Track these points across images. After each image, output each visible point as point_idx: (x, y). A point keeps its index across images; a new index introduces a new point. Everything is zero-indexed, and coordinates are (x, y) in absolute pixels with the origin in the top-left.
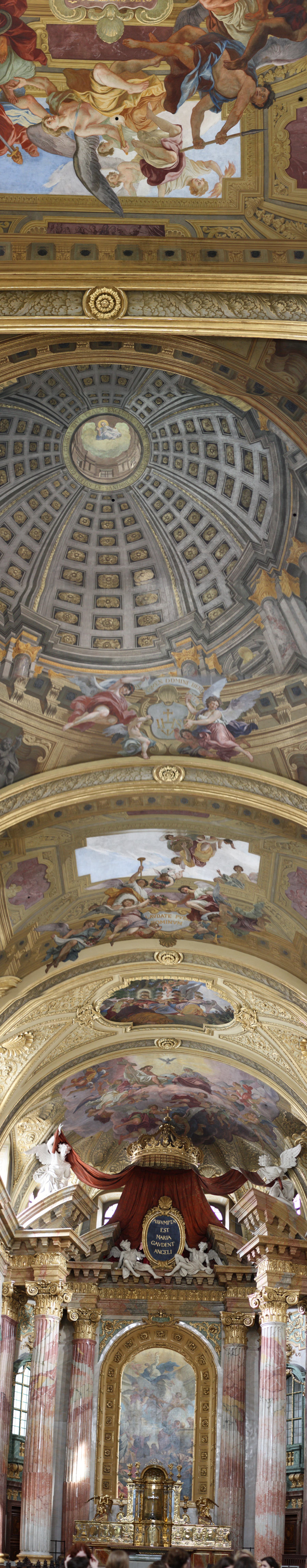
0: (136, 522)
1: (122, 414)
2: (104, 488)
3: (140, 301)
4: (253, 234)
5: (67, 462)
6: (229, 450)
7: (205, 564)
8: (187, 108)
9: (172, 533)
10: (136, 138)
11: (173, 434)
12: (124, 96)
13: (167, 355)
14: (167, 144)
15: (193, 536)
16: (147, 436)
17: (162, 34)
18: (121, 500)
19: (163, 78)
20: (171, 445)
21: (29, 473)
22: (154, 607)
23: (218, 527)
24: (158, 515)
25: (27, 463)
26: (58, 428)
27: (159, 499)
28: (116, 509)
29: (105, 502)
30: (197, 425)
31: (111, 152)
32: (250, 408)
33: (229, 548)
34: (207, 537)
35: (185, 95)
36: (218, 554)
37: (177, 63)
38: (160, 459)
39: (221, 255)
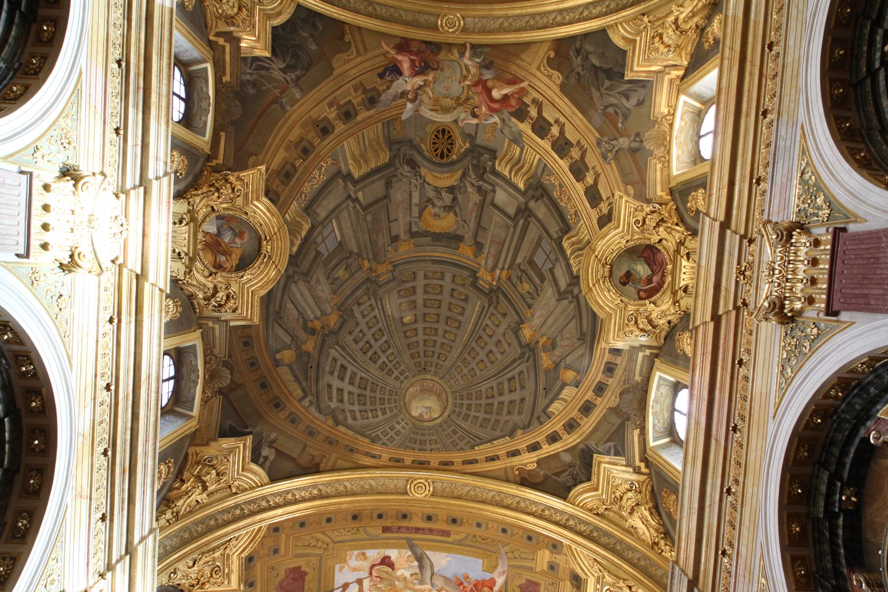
0: (411, 355)
1: (415, 421)
2: (429, 377)
3: (399, 488)
4: (330, 533)
5: (450, 395)
6: (351, 401)
7: (370, 328)
9: (389, 347)
11: (385, 409)
14: (378, 579)
15: (376, 346)
16: (401, 407)
18: (419, 369)
20: (386, 402)
21: (473, 391)
22: (403, 300)
23: (360, 352)
24: (397, 359)
25: (474, 398)
26: (453, 417)
27: (396, 369)
28: (423, 363)
29: (429, 368)
30: (370, 415)
31: (412, 575)
32: (337, 428)
33: (354, 340)
34: (367, 345)
36: (361, 335)
38: (394, 393)
39: (350, 517)
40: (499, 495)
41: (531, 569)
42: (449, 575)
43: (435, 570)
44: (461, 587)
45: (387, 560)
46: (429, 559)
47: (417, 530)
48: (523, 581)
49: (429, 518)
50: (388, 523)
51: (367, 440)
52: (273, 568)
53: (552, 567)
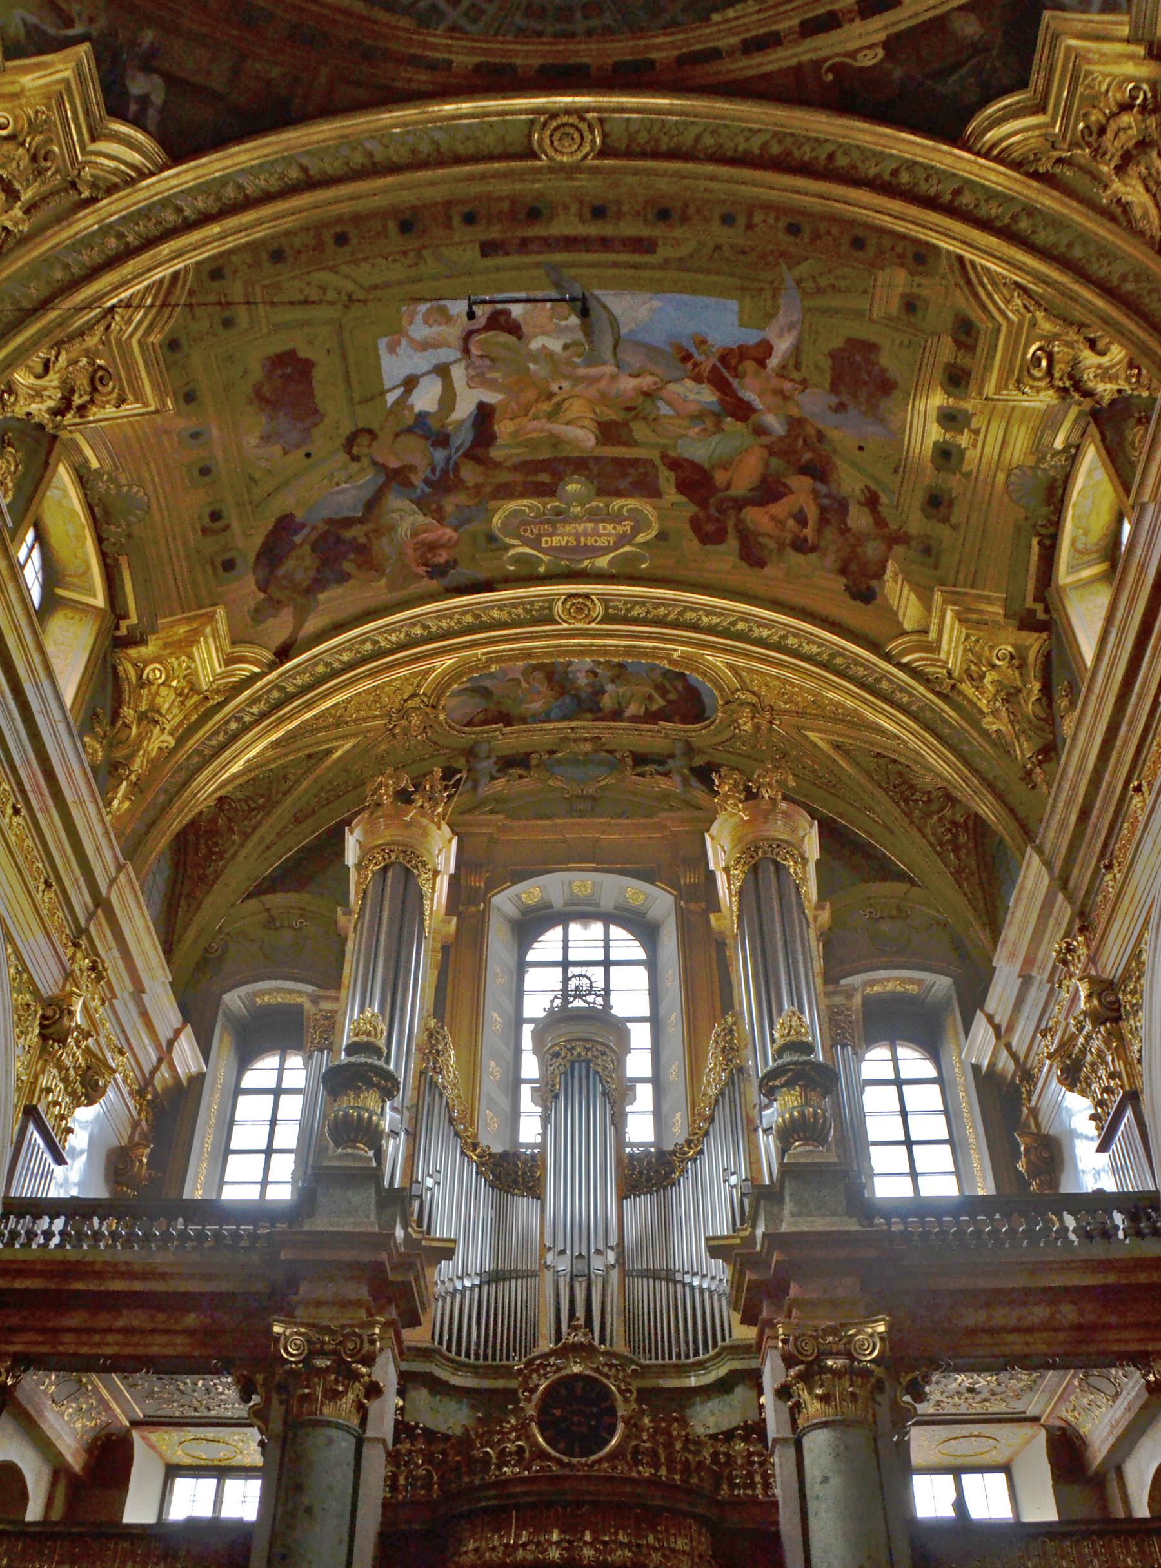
8: (464, 408)
10: (531, 366)
12: (552, 416)
13: (463, 60)
14: (488, 362)
17: (506, 492)
19: (499, 441)
31: (566, 347)
35: (468, 424)
37: (482, 461)
40: (780, 142)
41: (859, 314)
42: (658, 338)
43: (624, 331)
44: (690, 365)
45: (502, 319)
46: (605, 307)
47: (570, 243)
48: (838, 342)
49: (599, 212)
50: (495, 233)
51: (405, 22)
52: (230, 358)
53: (910, 305)
